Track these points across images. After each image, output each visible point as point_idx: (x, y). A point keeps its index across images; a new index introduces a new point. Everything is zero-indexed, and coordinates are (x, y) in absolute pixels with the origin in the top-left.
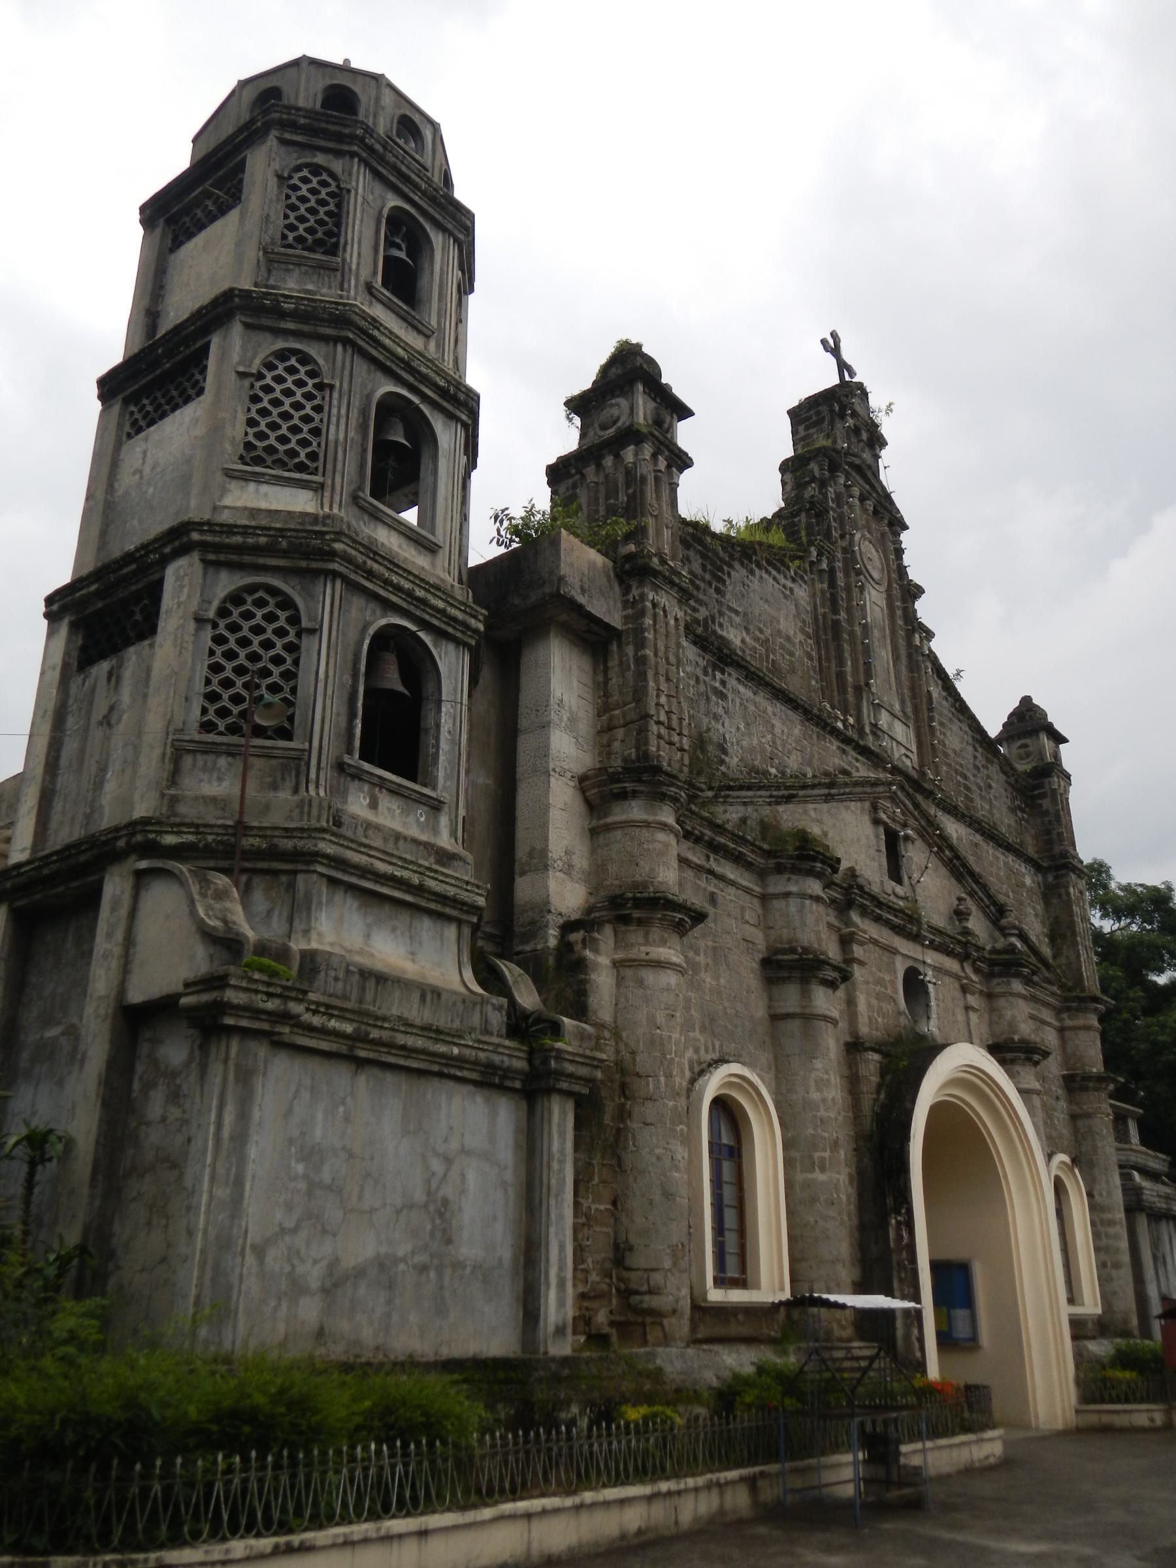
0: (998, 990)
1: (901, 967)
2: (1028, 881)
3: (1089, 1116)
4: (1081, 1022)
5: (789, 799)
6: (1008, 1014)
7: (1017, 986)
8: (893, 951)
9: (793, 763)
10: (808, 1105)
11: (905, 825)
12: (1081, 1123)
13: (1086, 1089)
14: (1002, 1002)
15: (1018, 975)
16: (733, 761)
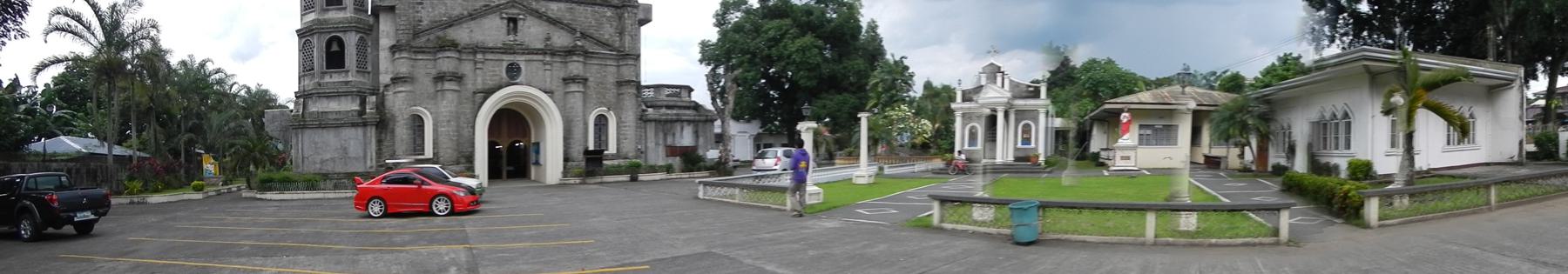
0: (568, 60)
1: (505, 64)
2: (609, 14)
3: (622, 94)
4: (625, 63)
5: (450, 26)
6: (571, 67)
7: (575, 58)
8: (503, 60)
9: (456, 13)
10: (442, 112)
11: (520, 14)
12: (621, 96)
13: (622, 85)
14: (569, 64)
15: (575, 54)
16: (425, 23)
